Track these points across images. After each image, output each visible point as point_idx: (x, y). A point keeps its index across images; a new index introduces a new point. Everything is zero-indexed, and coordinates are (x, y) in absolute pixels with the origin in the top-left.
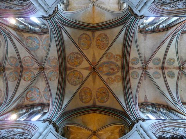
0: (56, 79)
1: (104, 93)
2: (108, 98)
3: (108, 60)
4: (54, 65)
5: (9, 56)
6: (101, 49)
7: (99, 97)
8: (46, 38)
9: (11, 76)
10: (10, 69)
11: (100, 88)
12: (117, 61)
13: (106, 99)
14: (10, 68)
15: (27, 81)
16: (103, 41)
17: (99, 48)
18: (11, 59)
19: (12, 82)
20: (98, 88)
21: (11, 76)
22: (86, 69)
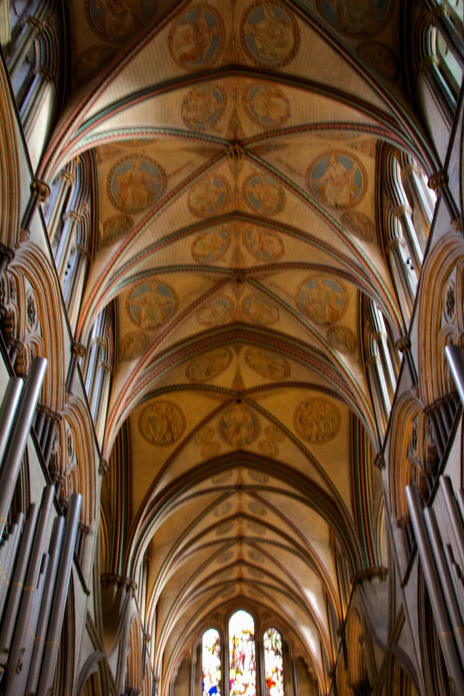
0: (204, 324)
1: (169, 428)
4: (252, 311)
7: (153, 412)
8: (345, 290)
10: (236, 172)
11: (181, 411)
12: (261, 445)
13: (153, 438)
15: (192, 250)
16: (317, 424)
17: (299, 408)
18: (275, 192)
19: (186, 205)
20: (181, 405)
22: (238, 379)
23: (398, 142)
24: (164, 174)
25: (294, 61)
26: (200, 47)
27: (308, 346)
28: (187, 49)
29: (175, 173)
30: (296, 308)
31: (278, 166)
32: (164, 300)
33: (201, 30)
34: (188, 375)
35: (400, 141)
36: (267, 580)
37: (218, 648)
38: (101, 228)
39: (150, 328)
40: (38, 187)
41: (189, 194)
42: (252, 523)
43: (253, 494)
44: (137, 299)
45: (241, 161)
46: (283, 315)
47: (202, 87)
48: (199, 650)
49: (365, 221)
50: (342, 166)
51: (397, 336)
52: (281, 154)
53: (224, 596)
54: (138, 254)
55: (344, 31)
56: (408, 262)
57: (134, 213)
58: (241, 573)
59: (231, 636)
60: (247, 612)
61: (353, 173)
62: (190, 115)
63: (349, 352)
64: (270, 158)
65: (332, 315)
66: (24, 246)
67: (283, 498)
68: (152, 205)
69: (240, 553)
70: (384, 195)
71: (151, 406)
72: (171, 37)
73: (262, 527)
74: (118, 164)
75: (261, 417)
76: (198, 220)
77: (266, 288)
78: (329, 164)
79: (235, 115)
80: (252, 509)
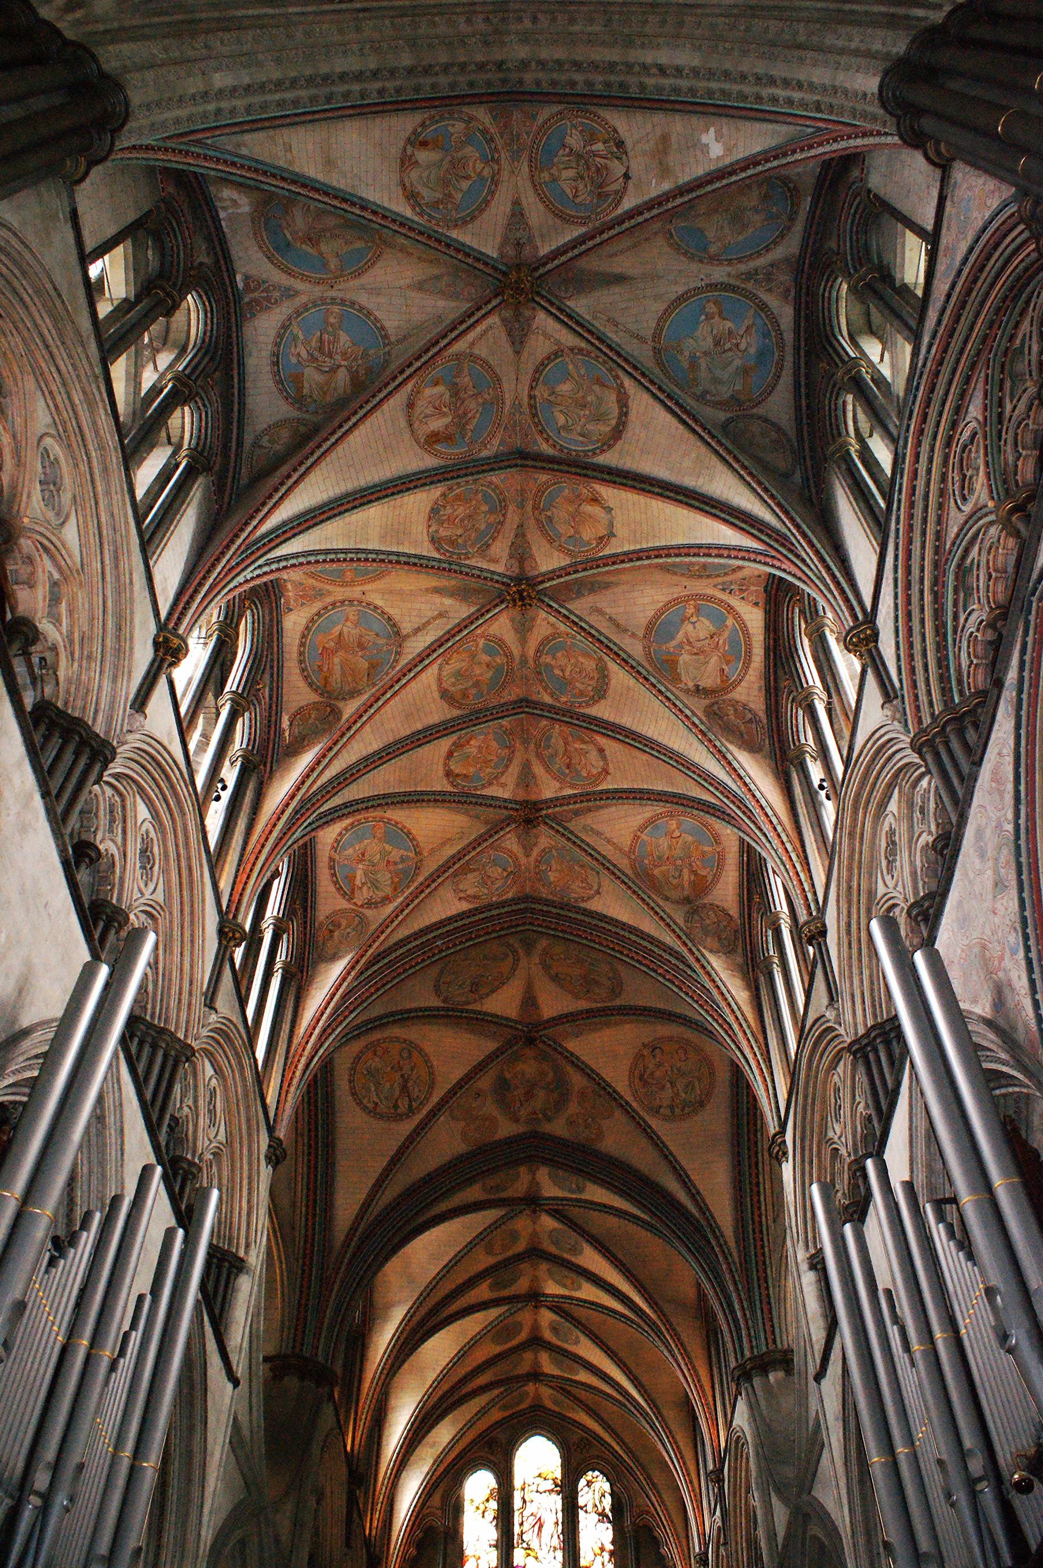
0: (466, 899)
1: (404, 1088)
2: (381, 1117)
3: (576, 1089)
4: (552, 876)
5: (613, 666)
6: (634, 1066)
9: (473, 656)
10: (523, 630)
12: (571, 1123)
13: (375, 1108)
14: (530, 629)
15: (446, 765)
17: (639, 1057)
18: (590, 665)
19: (434, 688)
20: (428, 1047)
21: (473, 656)
22: (529, 1001)
23: (800, 579)
24: (398, 633)
25: (620, 443)
26: (461, 421)
27: (651, 939)
28: (437, 424)
29: (417, 630)
30: (629, 872)
31: (593, 619)
32: (396, 854)
33: (462, 395)
34: (437, 990)
35: (799, 574)
36: (583, 1376)
37: (493, 1505)
38: (285, 723)
39: (370, 904)
40: (166, 640)
41: (440, 669)
42: (555, 1269)
43: (557, 1214)
44: (350, 851)
45: (531, 613)
46: (608, 883)
47: (463, 486)
48: (457, 1510)
49: (750, 716)
50: (707, 623)
51: (803, 916)
52: (601, 600)
53: (504, 1408)
54: (350, 768)
55: (701, 398)
56: (821, 787)
57: (344, 699)
58: (536, 1363)
59: (517, 1483)
60: (549, 1439)
61: (726, 634)
62: (443, 533)
63: (727, 950)
64: (580, 606)
65: (694, 885)
66: (134, 740)
67: (612, 1221)
68: (374, 685)
69: (536, 1327)
70: (780, 673)
71: (372, 1047)
72: (411, 405)
73: (574, 1276)
74: (318, 614)
75: (570, 1069)
76: (456, 713)
77: (577, 837)
78: (685, 619)
79: (520, 533)
80: (556, 1243)
